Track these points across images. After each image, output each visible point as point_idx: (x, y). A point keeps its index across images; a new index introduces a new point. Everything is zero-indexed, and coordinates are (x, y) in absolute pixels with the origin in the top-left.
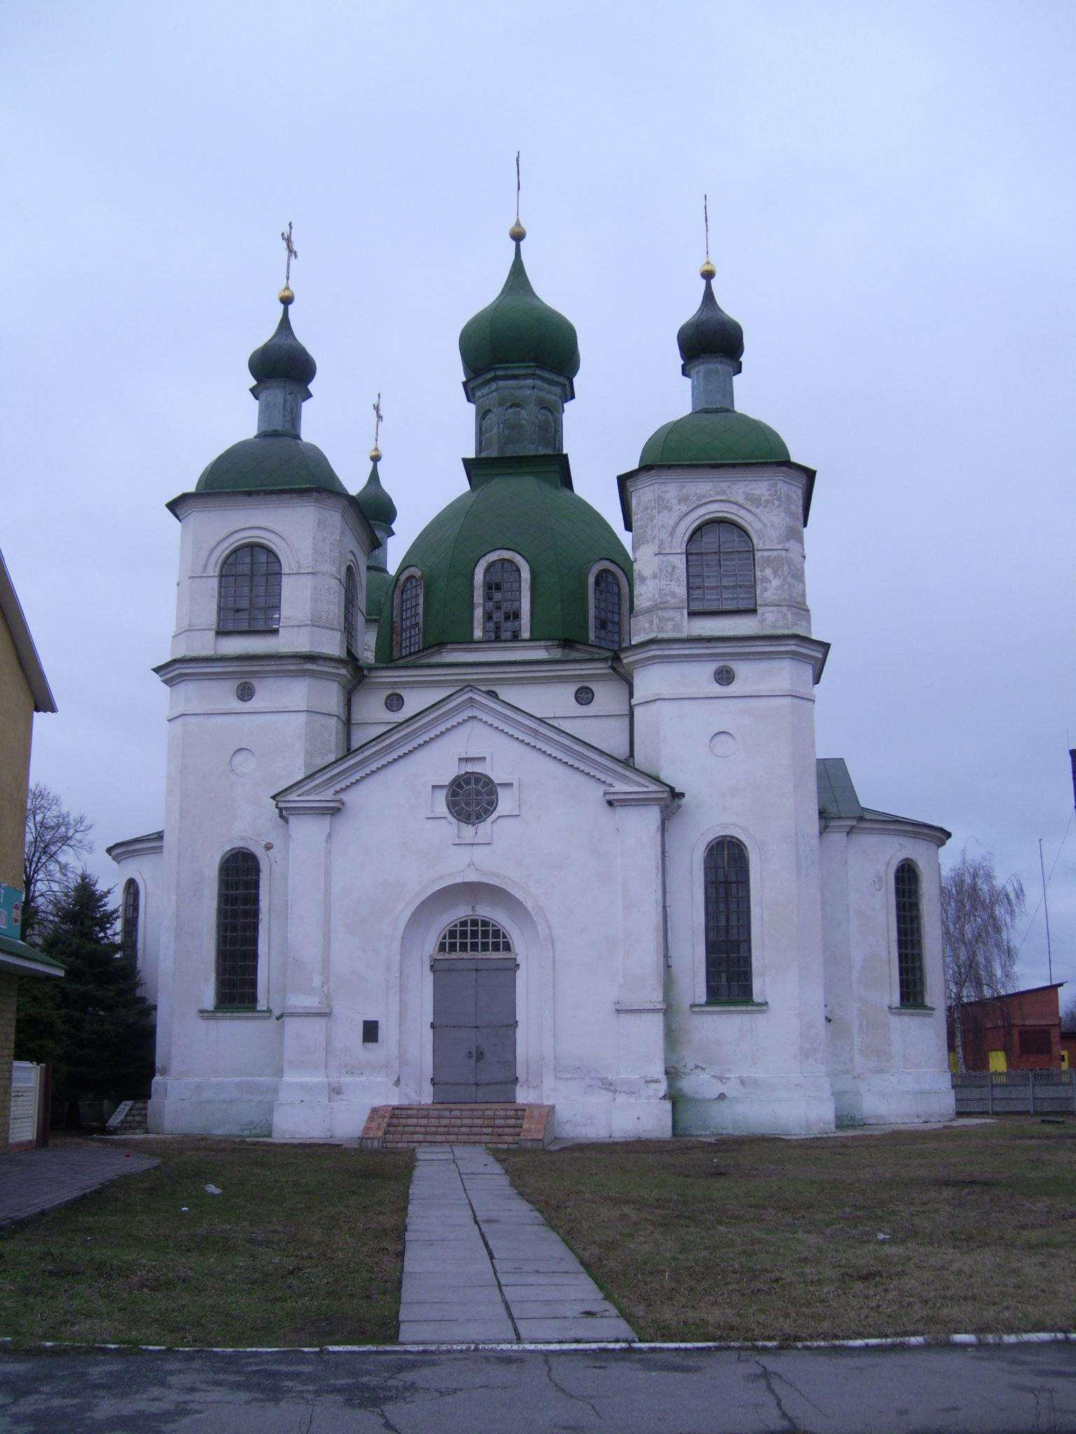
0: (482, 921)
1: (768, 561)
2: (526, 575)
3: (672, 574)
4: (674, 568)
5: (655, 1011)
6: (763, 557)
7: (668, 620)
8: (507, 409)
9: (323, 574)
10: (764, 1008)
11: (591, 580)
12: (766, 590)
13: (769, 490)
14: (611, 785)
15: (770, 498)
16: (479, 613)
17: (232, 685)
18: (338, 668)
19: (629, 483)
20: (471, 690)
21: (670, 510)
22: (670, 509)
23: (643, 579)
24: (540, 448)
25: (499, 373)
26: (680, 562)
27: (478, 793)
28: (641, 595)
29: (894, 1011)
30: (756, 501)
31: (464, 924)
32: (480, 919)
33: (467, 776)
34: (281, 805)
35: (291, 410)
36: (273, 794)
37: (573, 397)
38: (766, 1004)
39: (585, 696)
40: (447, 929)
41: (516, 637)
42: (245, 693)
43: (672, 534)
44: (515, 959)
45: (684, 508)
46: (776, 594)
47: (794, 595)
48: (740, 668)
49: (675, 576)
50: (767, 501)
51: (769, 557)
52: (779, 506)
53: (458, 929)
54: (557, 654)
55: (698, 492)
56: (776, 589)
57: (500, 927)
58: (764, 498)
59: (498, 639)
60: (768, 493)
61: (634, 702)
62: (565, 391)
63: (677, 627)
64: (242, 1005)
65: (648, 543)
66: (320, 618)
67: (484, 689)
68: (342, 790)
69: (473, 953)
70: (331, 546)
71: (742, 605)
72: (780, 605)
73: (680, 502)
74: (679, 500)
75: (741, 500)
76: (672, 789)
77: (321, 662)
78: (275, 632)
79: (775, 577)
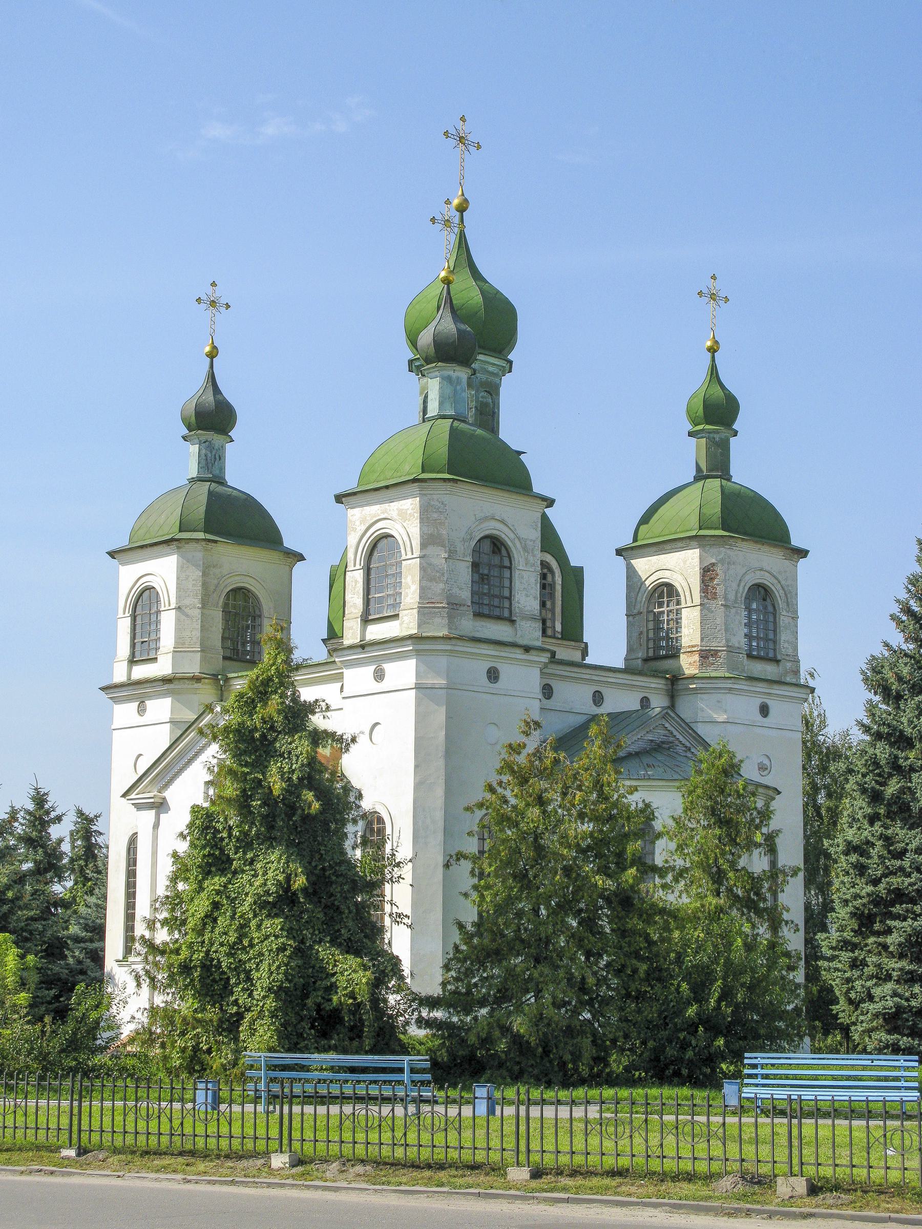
3: (355, 589)
4: (356, 582)
42: (141, 710)
45: (364, 528)
48: (388, 667)
66: (184, 644)
77: (176, 682)
78: (155, 660)
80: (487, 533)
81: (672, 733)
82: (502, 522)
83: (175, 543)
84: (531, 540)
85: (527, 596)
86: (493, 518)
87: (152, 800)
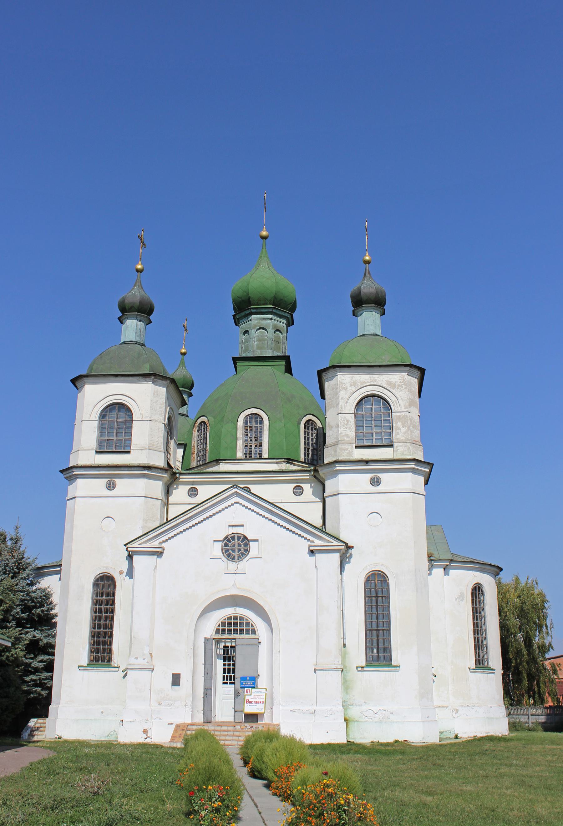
0: (240, 617)
1: (399, 418)
2: (266, 422)
3: (347, 425)
4: (348, 421)
5: (337, 669)
6: (396, 416)
7: (344, 450)
8: (256, 331)
10: (398, 668)
11: (302, 425)
12: (398, 434)
13: (399, 379)
14: (313, 542)
15: (401, 384)
16: (240, 443)
17: (103, 482)
18: (162, 473)
19: (324, 374)
20: (236, 488)
21: (346, 390)
22: (346, 389)
23: (331, 427)
24: (274, 352)
25: (253, 311)
26: (351, 418)
27: (239, 545)
28: (330, 436)
29: (471, 670)
30: (393, 385)
31: (230, 618)
32: (239, 615)
33: (233, 535)
34: (129, 549)
35: (140, 329)
36: (124, 544)
37: (293, 324)
38: (399, 667)
39: (298, 491)
40: (222, 620)
41: (260, 458)
42: (111, 486)
43: (346, 403)
44: (258, 639)
45: (354, 389)
46: (404, 436)
49: (348, 426)
50: (399, 385)
51: (400, 416)
52: (405, 388)
53: (227, 621)
54: (285, 466)
55: (362, 380)
56: (404, 433)
57: (250, 620)
58: (397, 384)
59: (251, 457)
60: (400, 381)
61: (325, 495)
62: (288, 321)
63: (350, 454)
64: (103, 663)
65: (334, 407)
67: (242, 486)
68: (164, 542)
69: (234, 635)
70: (161, 406)
71: (385, 442)
72: (406, 443)
73: (351, 386)
74: (351, 384)
75: (384, 386)
76: (346, 544)
77: (153, 470)
78: (129, 452)
79: (403, 427)
83: (153, 377)
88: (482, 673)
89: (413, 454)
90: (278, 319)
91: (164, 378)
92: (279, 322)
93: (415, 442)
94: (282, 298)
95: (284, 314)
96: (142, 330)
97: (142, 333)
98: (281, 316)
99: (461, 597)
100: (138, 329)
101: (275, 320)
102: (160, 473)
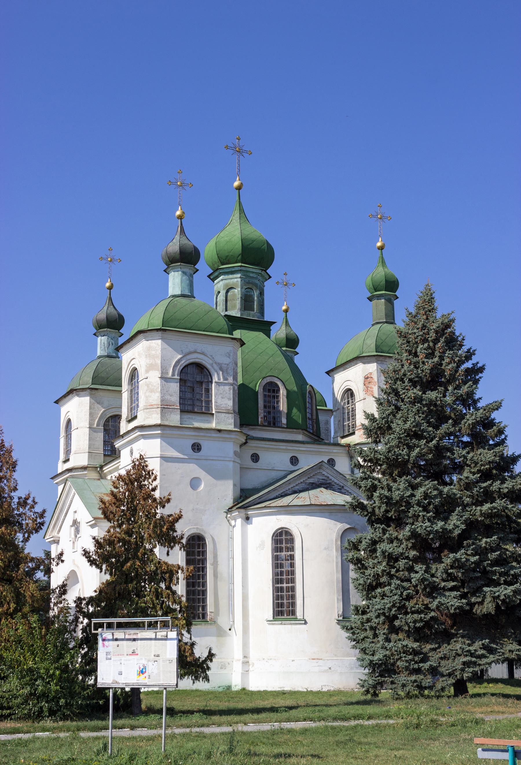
9: (81, 428)
18: (83, 471)
47: (150, 401)
66: (80, 449)
80: (191, 361)
81: (328, 477)
82: (203, 353)
83: (75, 392)
84: (225, 364)
85: (222, 398)
86: (195, 352)
87: (52, 539)
88: (281, 624)
89: (144, 420)
90: (231, 276)
91: (83, 390)
92: (231, 279)
93: (149, 407)
94: (227, 254)
95: (233, 270)
96: (106, 343)
97: (106, 345)
98: (232, 273)
99: (262, 545)
100: (102, 343)
101: (225, 279)
102: (81, 472)
